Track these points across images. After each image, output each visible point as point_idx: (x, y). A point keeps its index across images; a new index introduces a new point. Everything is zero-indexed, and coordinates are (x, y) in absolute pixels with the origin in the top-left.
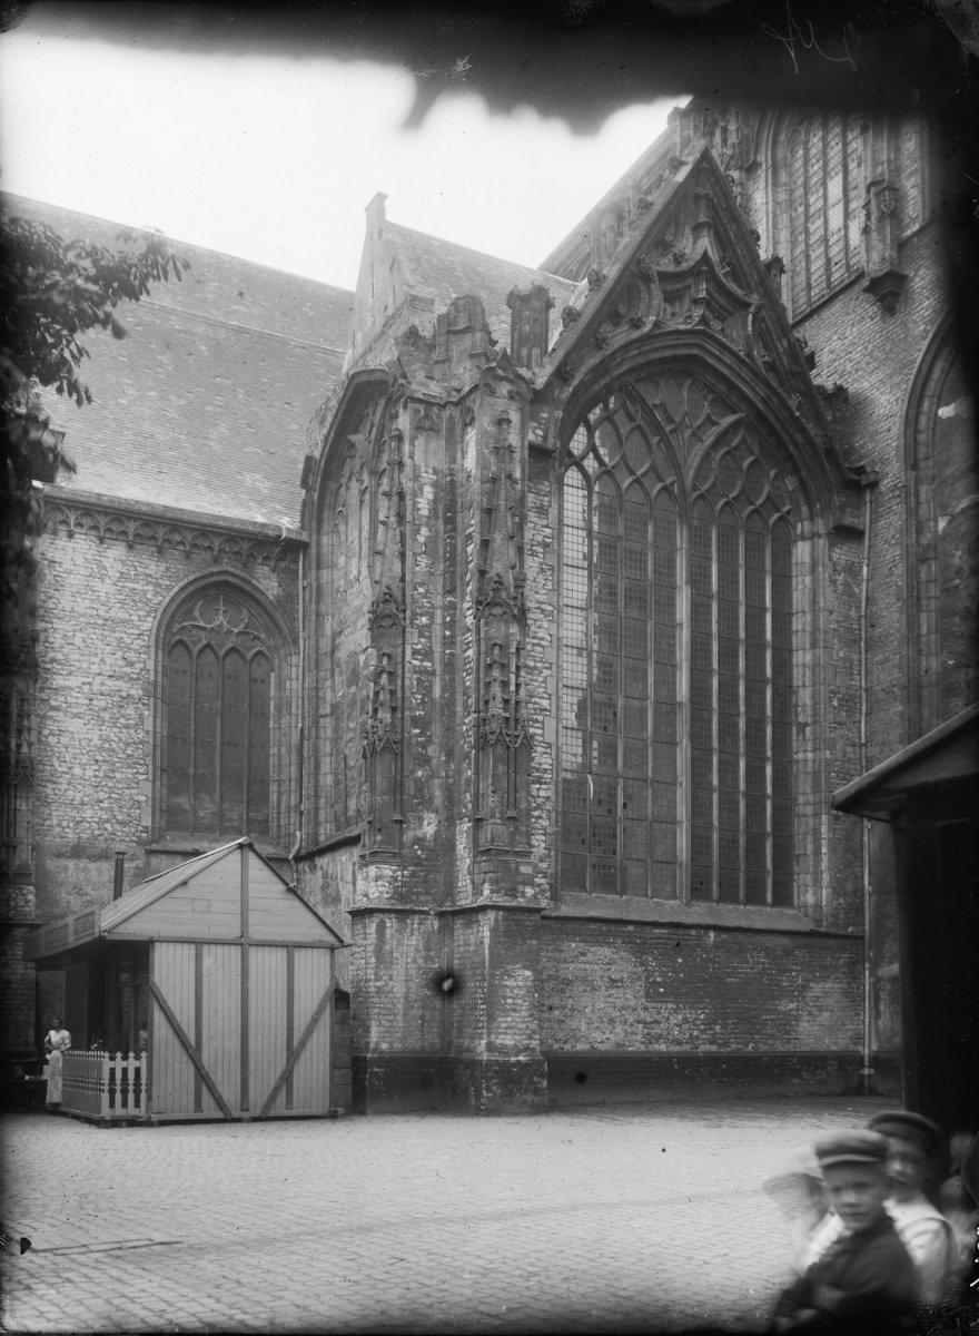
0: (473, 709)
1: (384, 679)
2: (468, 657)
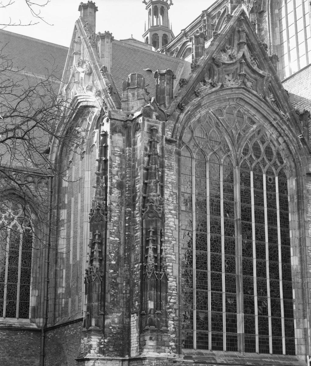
0: (139, 261)
1: (96, 246)
2: (137, 236)
